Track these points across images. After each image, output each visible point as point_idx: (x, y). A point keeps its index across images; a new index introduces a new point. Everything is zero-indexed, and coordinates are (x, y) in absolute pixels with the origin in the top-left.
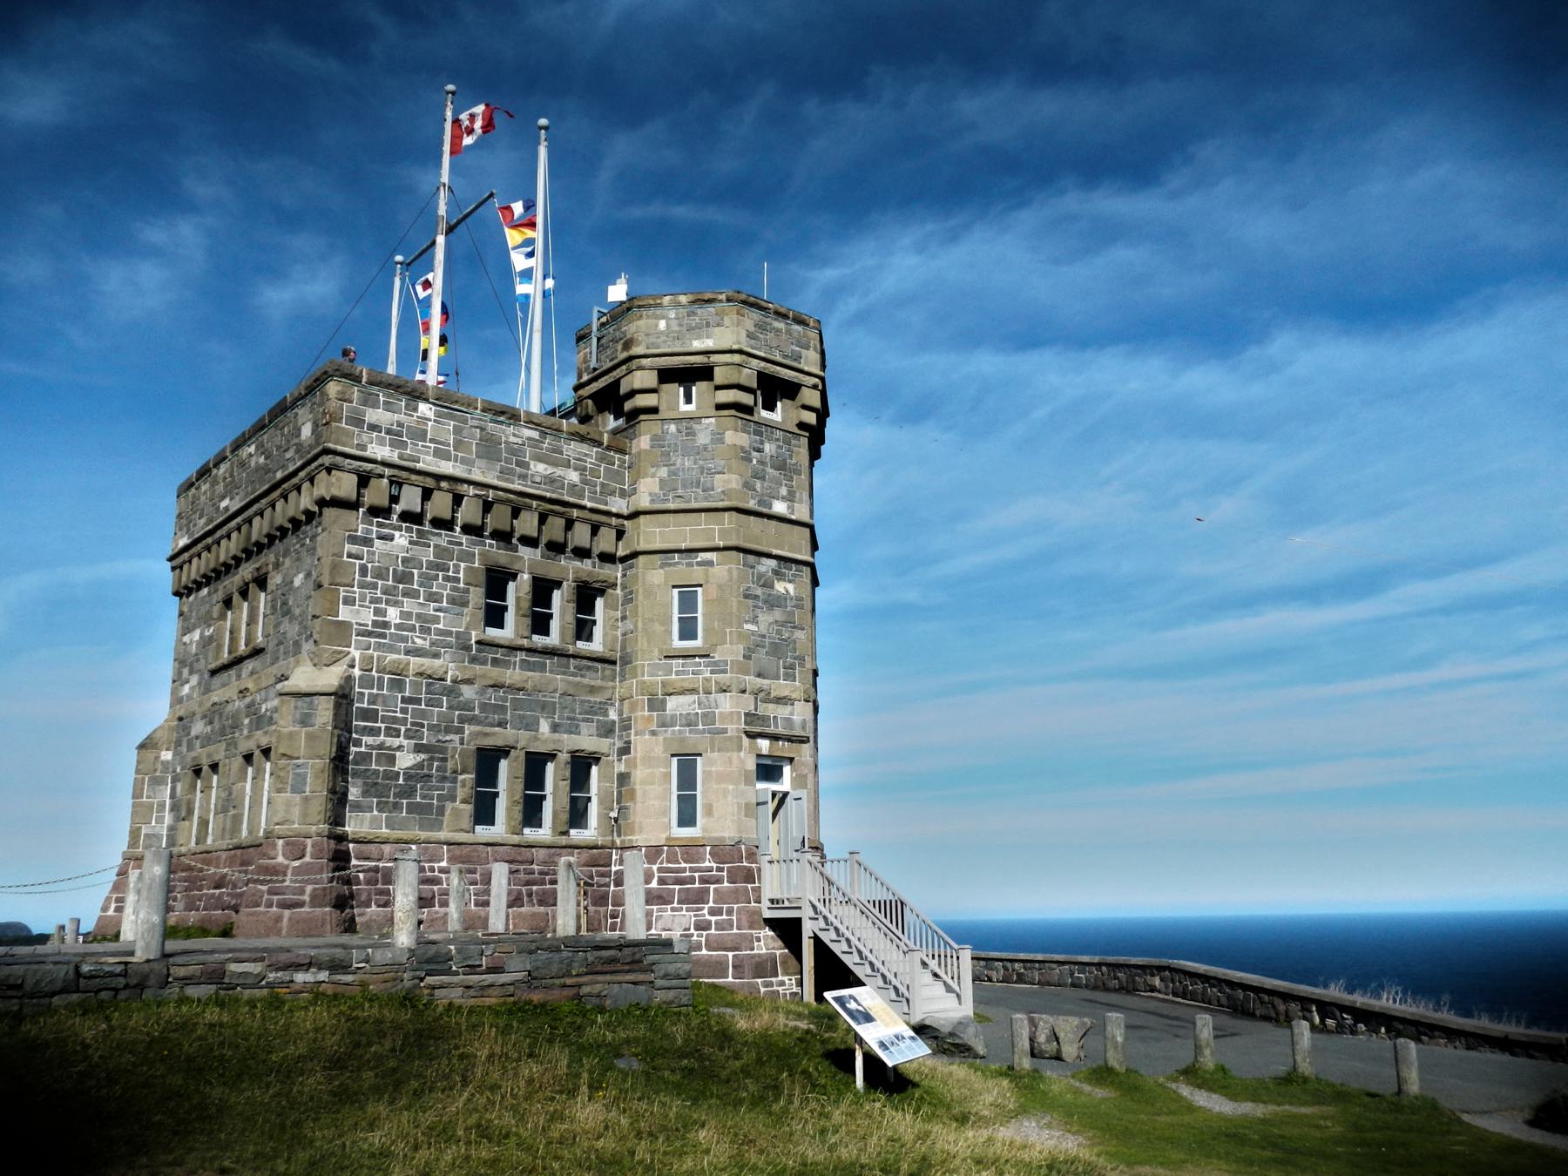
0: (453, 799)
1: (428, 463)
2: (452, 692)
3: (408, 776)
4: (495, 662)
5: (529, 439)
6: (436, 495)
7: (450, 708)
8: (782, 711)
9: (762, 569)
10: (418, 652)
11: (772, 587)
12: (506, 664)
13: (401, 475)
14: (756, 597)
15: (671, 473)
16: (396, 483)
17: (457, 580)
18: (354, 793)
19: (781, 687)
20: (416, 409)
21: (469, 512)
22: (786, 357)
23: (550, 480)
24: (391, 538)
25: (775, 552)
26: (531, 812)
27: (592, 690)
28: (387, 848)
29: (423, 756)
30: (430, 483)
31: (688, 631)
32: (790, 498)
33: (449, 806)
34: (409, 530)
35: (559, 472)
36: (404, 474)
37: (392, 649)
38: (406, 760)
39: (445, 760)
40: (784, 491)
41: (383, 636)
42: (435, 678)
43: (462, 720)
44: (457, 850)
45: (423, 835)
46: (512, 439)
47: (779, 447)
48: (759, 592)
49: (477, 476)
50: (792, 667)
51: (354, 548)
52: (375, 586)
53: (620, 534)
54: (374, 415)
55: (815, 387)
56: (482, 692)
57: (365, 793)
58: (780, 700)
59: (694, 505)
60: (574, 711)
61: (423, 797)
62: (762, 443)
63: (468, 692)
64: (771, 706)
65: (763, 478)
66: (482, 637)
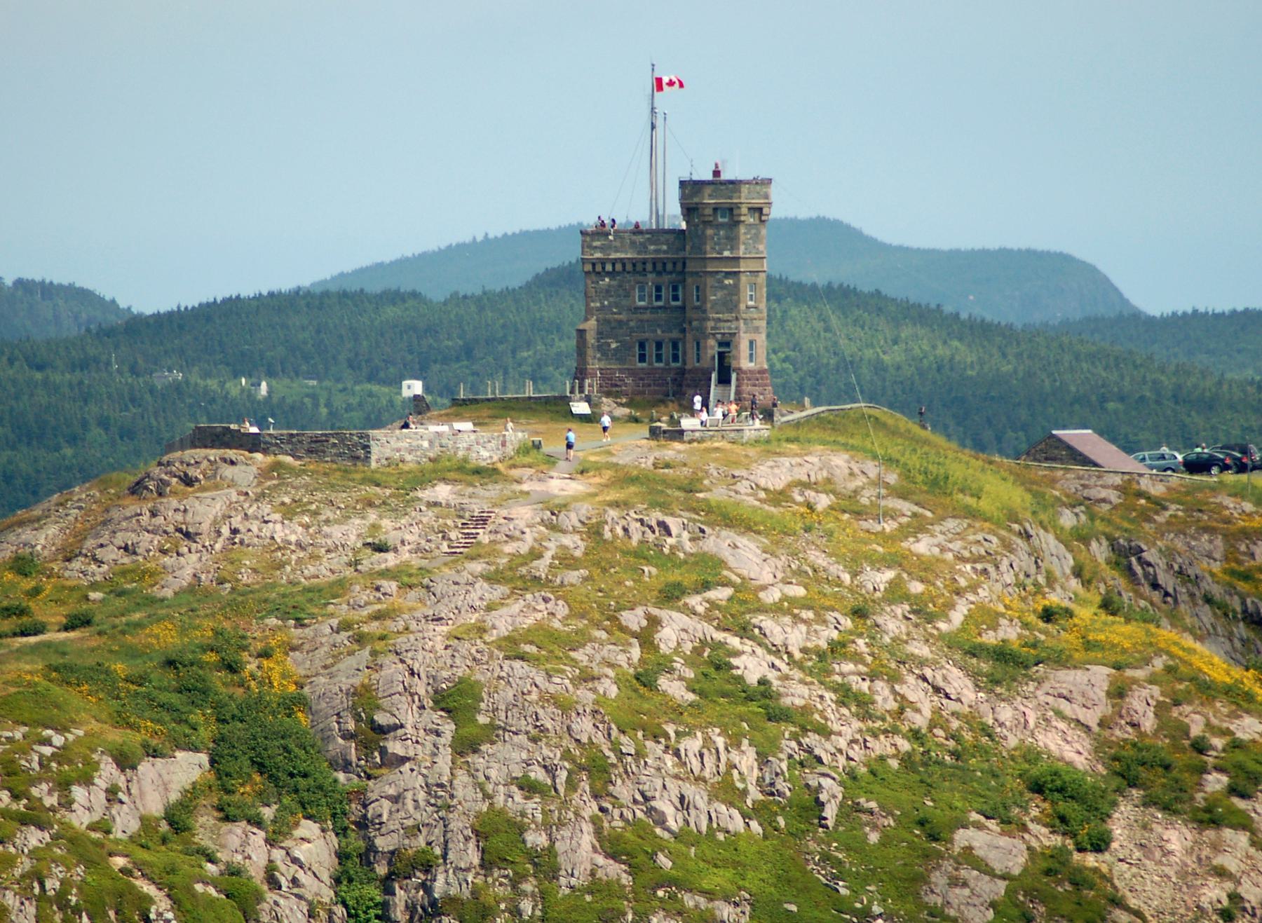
1: (613, 256)
3: (616, 349)
13: (603, 262)
19: (726, 316)
21: (629, 267)
23: (657, 251)
26: (659, 358)
32: (732, 249)
38: (614, 346)
42: (620, 322)
53: (684, 264)
63: (632, 324)
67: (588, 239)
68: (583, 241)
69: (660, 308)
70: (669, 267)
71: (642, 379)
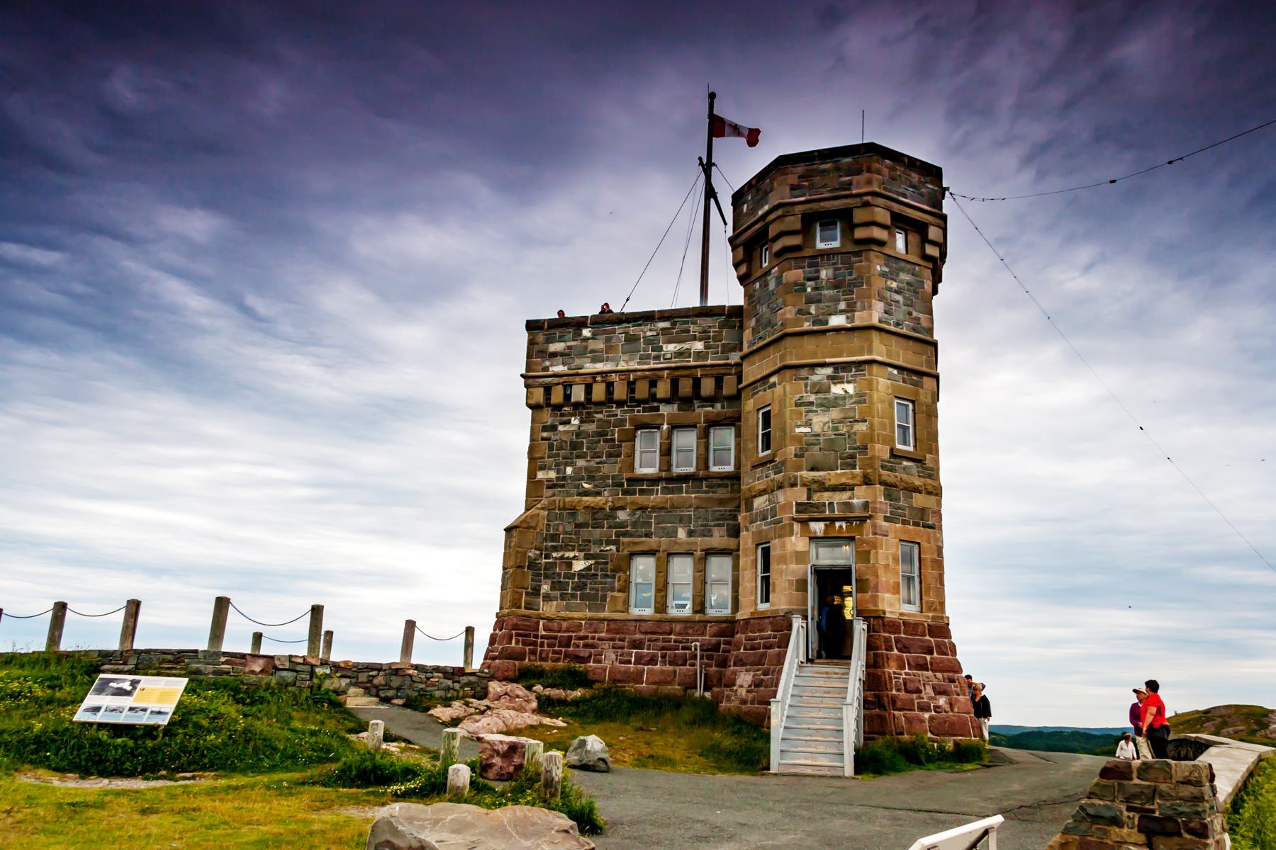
0: (613, 590)
1: (590, 367)
2: (611, 516)
3: (581, 574)
4: (642, 492)
5: (663, 329)
6: (595, 386)
7: (610, 527)
8: (844, 497)
9: (815, 378)
10: (586, 493)
11: (828, 390)
12: (650, 492)
14: (811, 403)
15: (757, 321)
16: (567, 386)
17: (613, 440)
18: (545, 588)
20: (580, 334)
21: (620, 392)
22: (831, 191)
23: (679, 354)
24: (569, 422)
25: (828, 360)
27: (722, 502)
28: (565, 624)
29: (591, 562)
30: (589, 380)
31: (767, 446)
32: (850, 309)
33: (609, 594)
34: (580, 414)
35: (686, 346)
36: (571, 379)
37: (568, 494)
38: (579, 566)
39: (606, 563)
40: (842, 306)
41: (563, 486)
42: (595, 511)
43: (618, 535)
44: (613, 626)
45: (589, 614)
46: (649, 333)
47: (836, 269)
48: (812, 398)
49: (622, 366)
50: (852, 457)
51: (545, 435)
52: (558, 455)
54: (554, 347)
55: (867, 205)
56: (632, 514)
57: (553, 588)
58: (835, 489)
59: (768, 340)
60: (706, 519)
61: (592, 589)
62: (818, 271)
63: (622, 516)
64: (826, 494)
65: (819, 301)
66: (630, 475)
67: (541, 337)
68: (531, 343)
69: (685, 478)
70: (708, 387)
71: (637, 645)
